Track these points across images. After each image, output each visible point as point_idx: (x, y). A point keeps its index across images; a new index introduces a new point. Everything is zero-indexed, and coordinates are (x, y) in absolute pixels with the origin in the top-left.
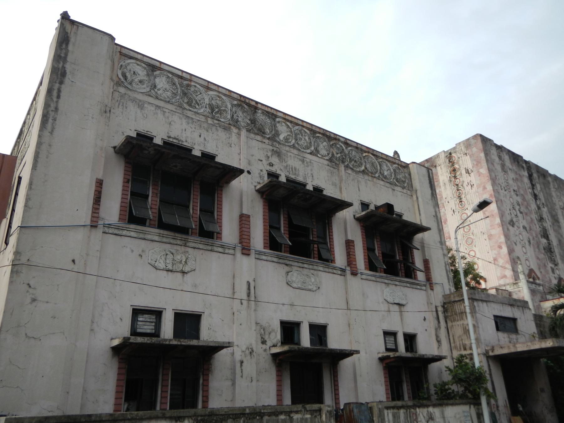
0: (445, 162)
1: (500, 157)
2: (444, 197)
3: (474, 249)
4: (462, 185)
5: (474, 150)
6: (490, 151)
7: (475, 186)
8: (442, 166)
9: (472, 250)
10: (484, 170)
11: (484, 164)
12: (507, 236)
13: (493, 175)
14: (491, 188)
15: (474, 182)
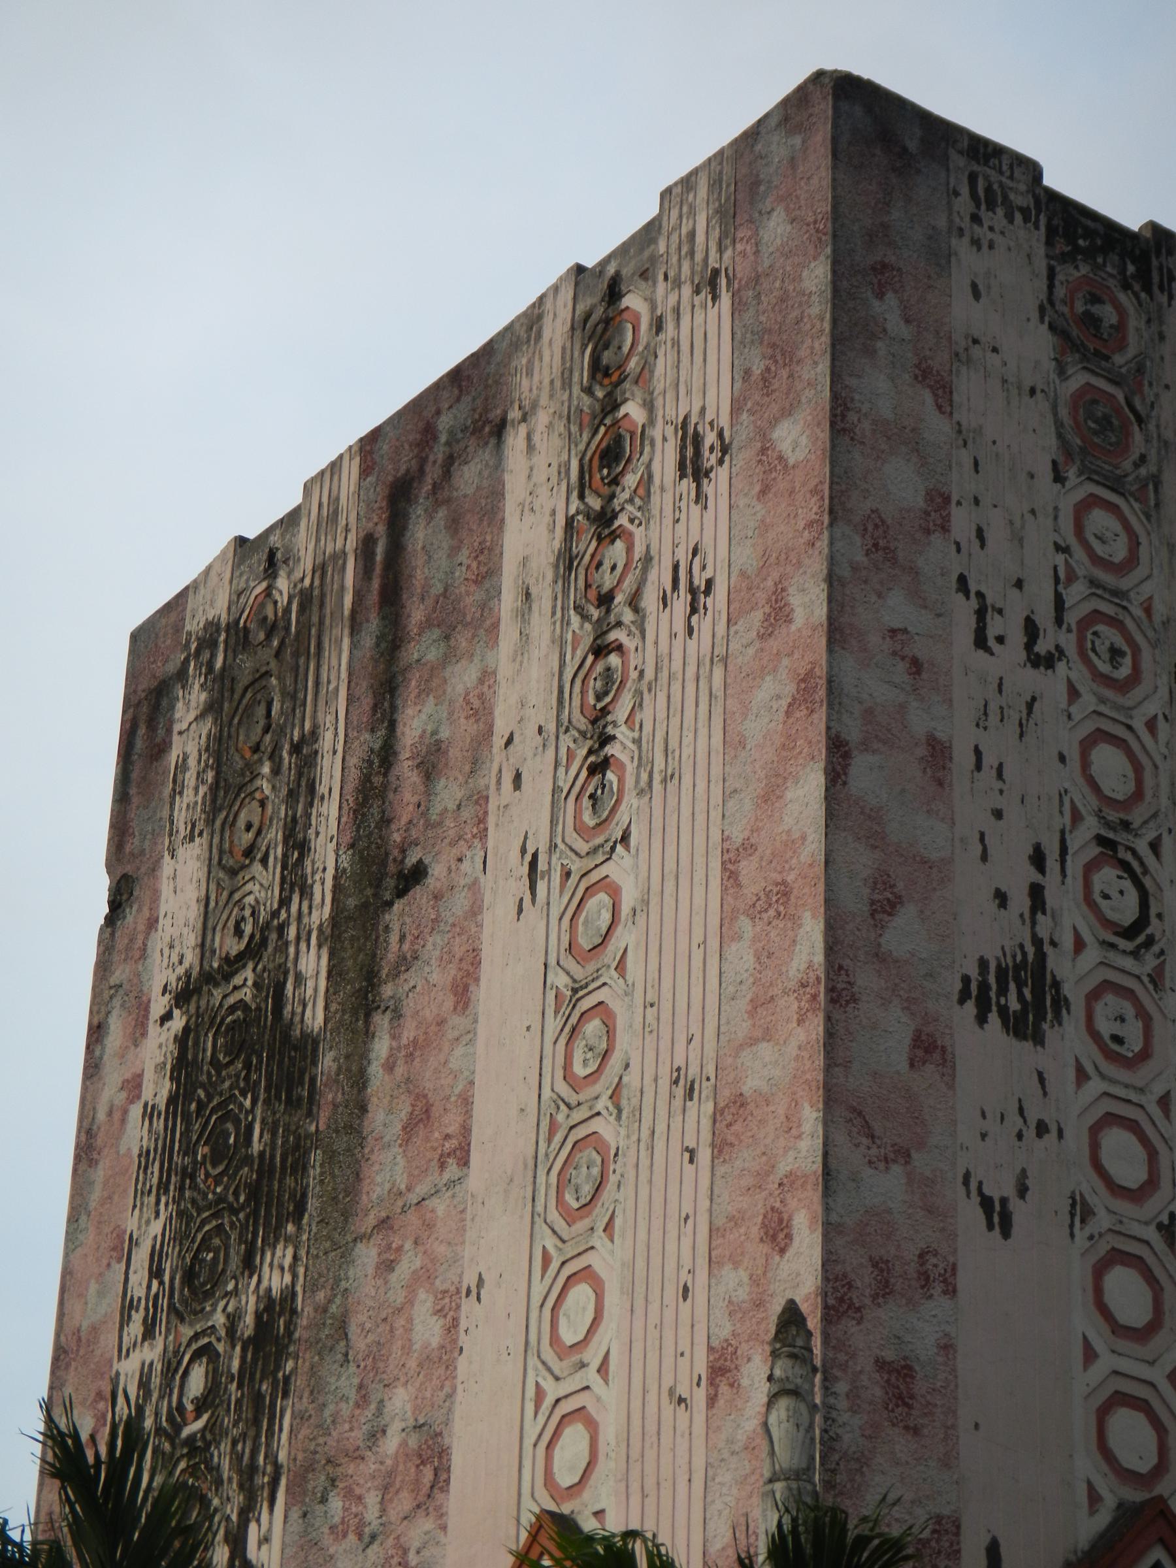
0: (567, 383)
1: (1080, 337)
2: (501, 729)
3: (606, 1259)
4: (634, 602)
5: (777, 228)
6: (940, 259)
7: (720, 589)
8: (542, 418)
9: (586, 1274)
10: (799, 438)
11: (815, 371)
12: (861, 1117)
13: (900, 485)
14: (821, 612)
15: (718, 565)
